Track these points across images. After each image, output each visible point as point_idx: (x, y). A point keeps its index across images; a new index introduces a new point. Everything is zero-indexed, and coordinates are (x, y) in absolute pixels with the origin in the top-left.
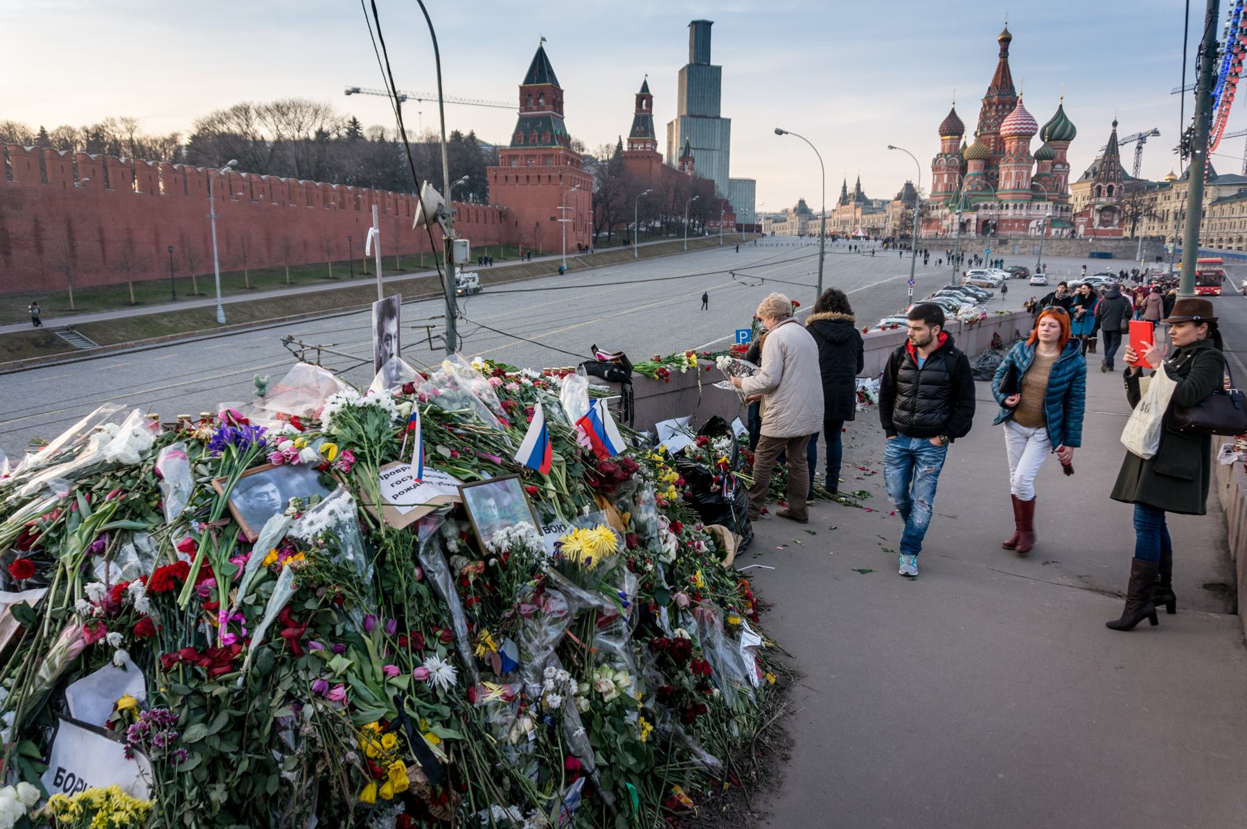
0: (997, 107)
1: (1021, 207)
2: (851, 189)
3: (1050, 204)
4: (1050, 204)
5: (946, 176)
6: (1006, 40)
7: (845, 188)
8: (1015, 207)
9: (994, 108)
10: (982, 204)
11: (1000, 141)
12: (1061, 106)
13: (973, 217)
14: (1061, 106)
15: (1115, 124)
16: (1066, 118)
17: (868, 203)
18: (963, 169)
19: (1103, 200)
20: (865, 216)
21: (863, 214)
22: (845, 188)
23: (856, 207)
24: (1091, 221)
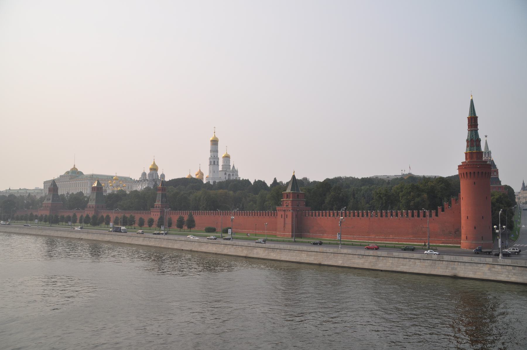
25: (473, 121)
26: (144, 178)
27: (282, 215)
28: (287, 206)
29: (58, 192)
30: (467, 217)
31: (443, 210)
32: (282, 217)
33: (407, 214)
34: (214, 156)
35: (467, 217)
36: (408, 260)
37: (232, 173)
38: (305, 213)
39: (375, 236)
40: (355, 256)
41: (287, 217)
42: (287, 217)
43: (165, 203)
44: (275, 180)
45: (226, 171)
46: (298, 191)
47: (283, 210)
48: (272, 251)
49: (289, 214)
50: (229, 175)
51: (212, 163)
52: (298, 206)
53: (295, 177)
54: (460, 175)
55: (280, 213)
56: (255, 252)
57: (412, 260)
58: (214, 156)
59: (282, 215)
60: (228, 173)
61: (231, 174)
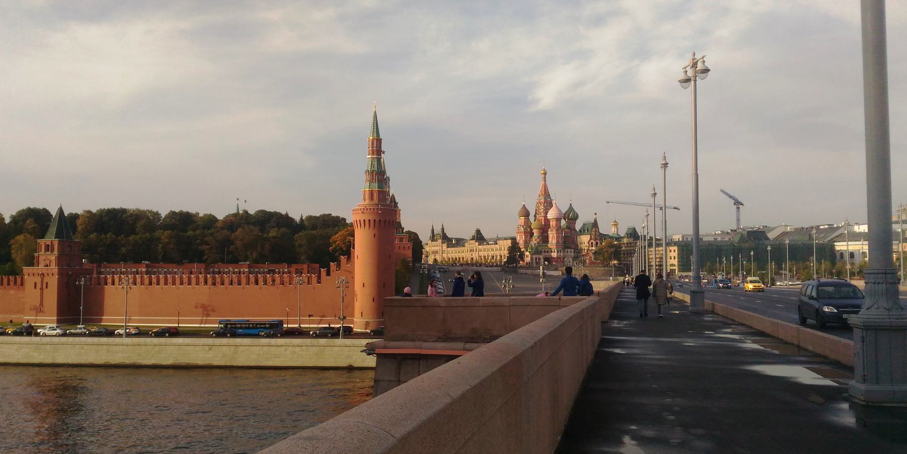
0: (544, 204)
1: (561, 251)
2: (438, 230)
3: (572, 250)
4: (572, 250)
5: (524, 236)
6: (545, 174)
7: (433, 230)
8: (558, 252)
9: (542, 205)
10: (543, 250)
11: (547, 221)
12: (571, 204)
13: (541, 257)
14: (571, 204)
15: (596, 214)
16: (574, 210)
17: (450, 240)
18: (532, 234)
19: (594, 248)
20: (448, 249)
21: (448, 247)
22: (433, 230)
23: (443, 243)
24: (591, 257)
25: (377, 149)
27: (35, 283)
28: (47, 266)
30: (364, 284)
31: (328, 274)
32: (35, 288)
33: (274, 281)
35: (364, 284)
36: (283, 348)
38: (106, 278)
40: (197, 348)
41: (47, 287)
42: (47, 287)
47: (38, 274)
49: (53, 282)
53: (63, 212)
54: (355, 222)
55: (29, 281)
57: (290, 349)
59: (35, 283)
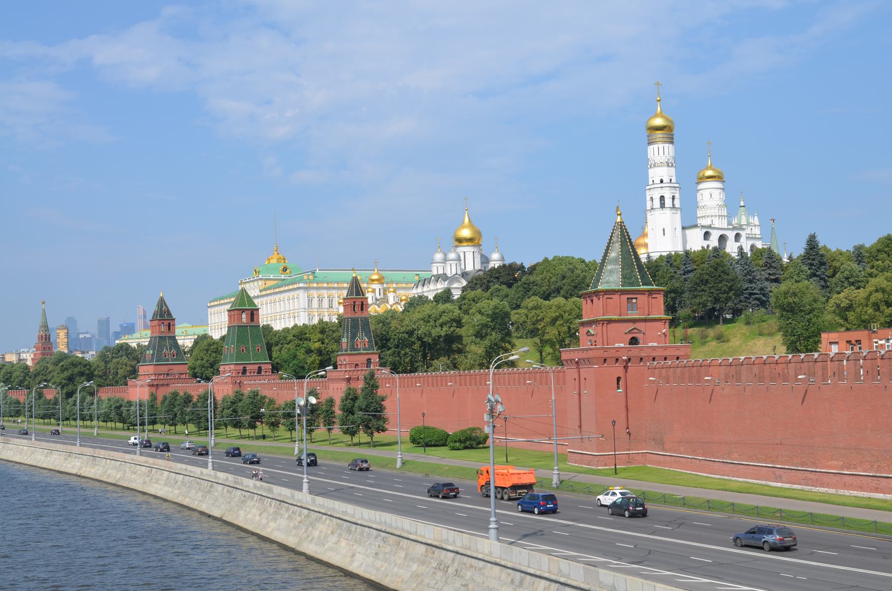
26: (441, 272)
29: (174, 332)
34: (662, 181)
37: (735, 232)
39: (842, 468)
43: (365, 349)
44: (812, 243)
45: (710, 227)
46: (632, 284)
48: (349, 531)
50: (722, 239)
51: (657, 203)
52: (634, 341)
56: (316, 534)
58: (662, 181)
60: (715, 236)
61: (731, 235)
